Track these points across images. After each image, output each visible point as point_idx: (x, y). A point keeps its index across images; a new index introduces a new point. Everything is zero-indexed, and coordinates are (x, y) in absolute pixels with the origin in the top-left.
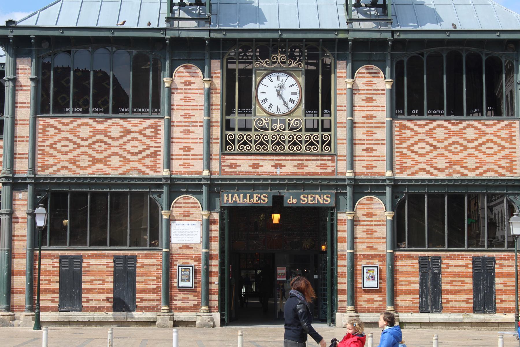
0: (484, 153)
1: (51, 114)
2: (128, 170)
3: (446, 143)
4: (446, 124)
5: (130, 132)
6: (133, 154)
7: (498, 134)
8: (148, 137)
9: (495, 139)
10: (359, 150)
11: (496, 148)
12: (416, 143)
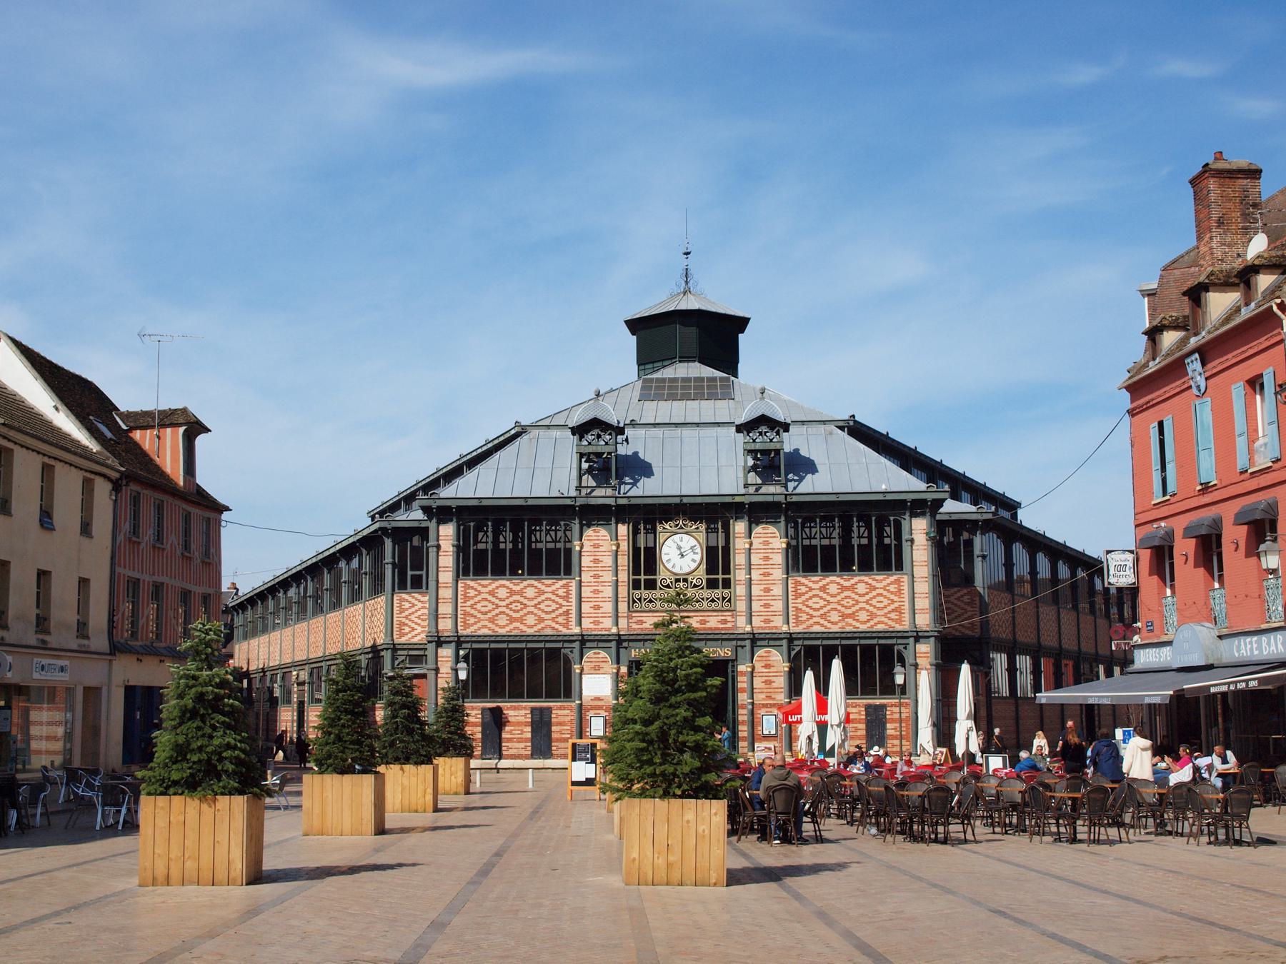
0: (875, 607)
1: (471, 577)
2: (543, 628)
3: (839, 598)
4: (838, 579)
5: (544, 593)
6: (547, 613)
7: (888, 588)
8: (561, 597)
9: (885, 593)
10: (756, 606)
11: (886, 602)
12: (811, 598)
